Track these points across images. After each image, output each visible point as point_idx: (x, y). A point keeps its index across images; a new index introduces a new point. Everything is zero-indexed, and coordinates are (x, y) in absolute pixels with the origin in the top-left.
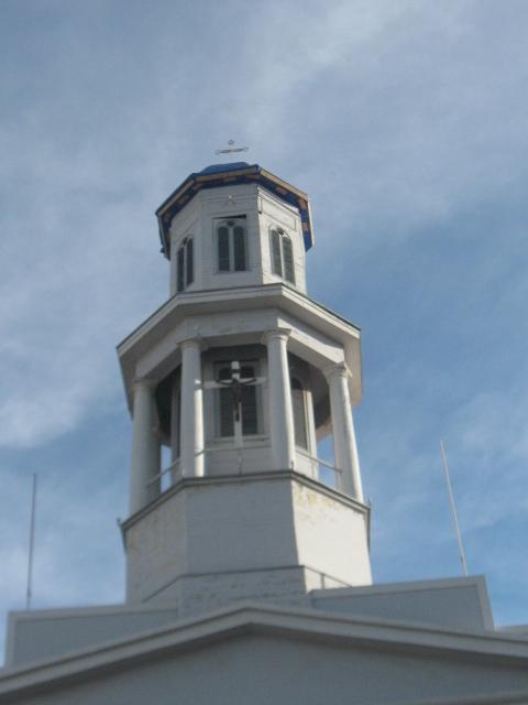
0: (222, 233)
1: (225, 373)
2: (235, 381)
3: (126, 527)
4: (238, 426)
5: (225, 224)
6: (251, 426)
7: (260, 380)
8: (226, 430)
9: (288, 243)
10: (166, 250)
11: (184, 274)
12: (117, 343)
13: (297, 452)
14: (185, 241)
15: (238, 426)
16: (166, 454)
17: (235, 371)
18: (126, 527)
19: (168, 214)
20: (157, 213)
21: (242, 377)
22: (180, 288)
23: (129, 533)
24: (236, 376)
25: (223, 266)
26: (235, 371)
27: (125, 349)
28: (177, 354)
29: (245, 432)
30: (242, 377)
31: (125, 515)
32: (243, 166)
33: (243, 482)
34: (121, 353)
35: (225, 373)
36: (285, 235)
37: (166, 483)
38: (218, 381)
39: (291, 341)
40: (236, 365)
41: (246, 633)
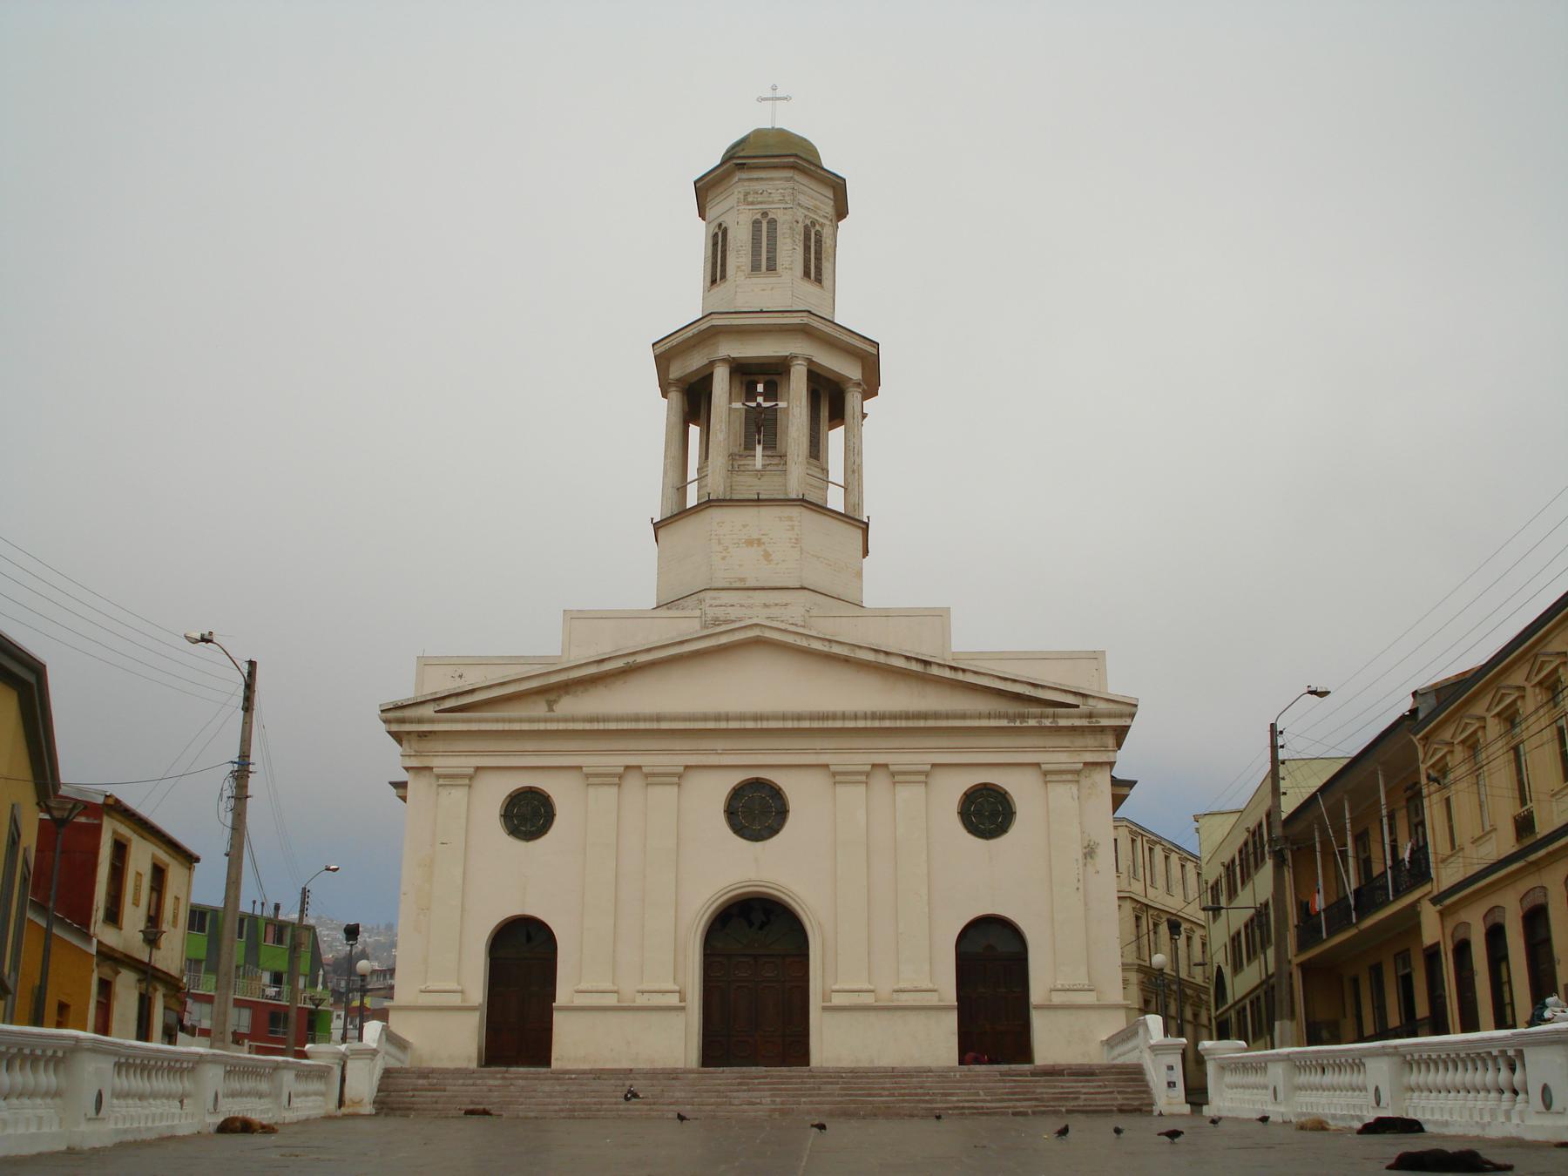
0: (756, 224)
1: (751, 394)
2: (759, 405)
3: (657, 527)
4: (759, 449)
5: (759, 216)
6: (771, 444)
7: (782, 404)
8: (749, 446)
10: (702, 214)
11: (717, 273)
14: (720, 225)
15: (759, 449)
16: (694, 431)
17: (760, 394)
18: (657, 527)
19: (706, 189)
21: (765, 401)
22: (713, 282)
23: (661, 533)
24: (760, 399)
25: (755, 267)
26: (760, 394)
27: (661, 348)
28: (712, 364)
29: (764, 448)
30: (765, 401)
32: (783, 136)
34: (658, 351)
35: (751, 394)
37: (692, 500)
38: (743, 404)
39: (810, 361)
40: (760, 388)
41: (758, 642)
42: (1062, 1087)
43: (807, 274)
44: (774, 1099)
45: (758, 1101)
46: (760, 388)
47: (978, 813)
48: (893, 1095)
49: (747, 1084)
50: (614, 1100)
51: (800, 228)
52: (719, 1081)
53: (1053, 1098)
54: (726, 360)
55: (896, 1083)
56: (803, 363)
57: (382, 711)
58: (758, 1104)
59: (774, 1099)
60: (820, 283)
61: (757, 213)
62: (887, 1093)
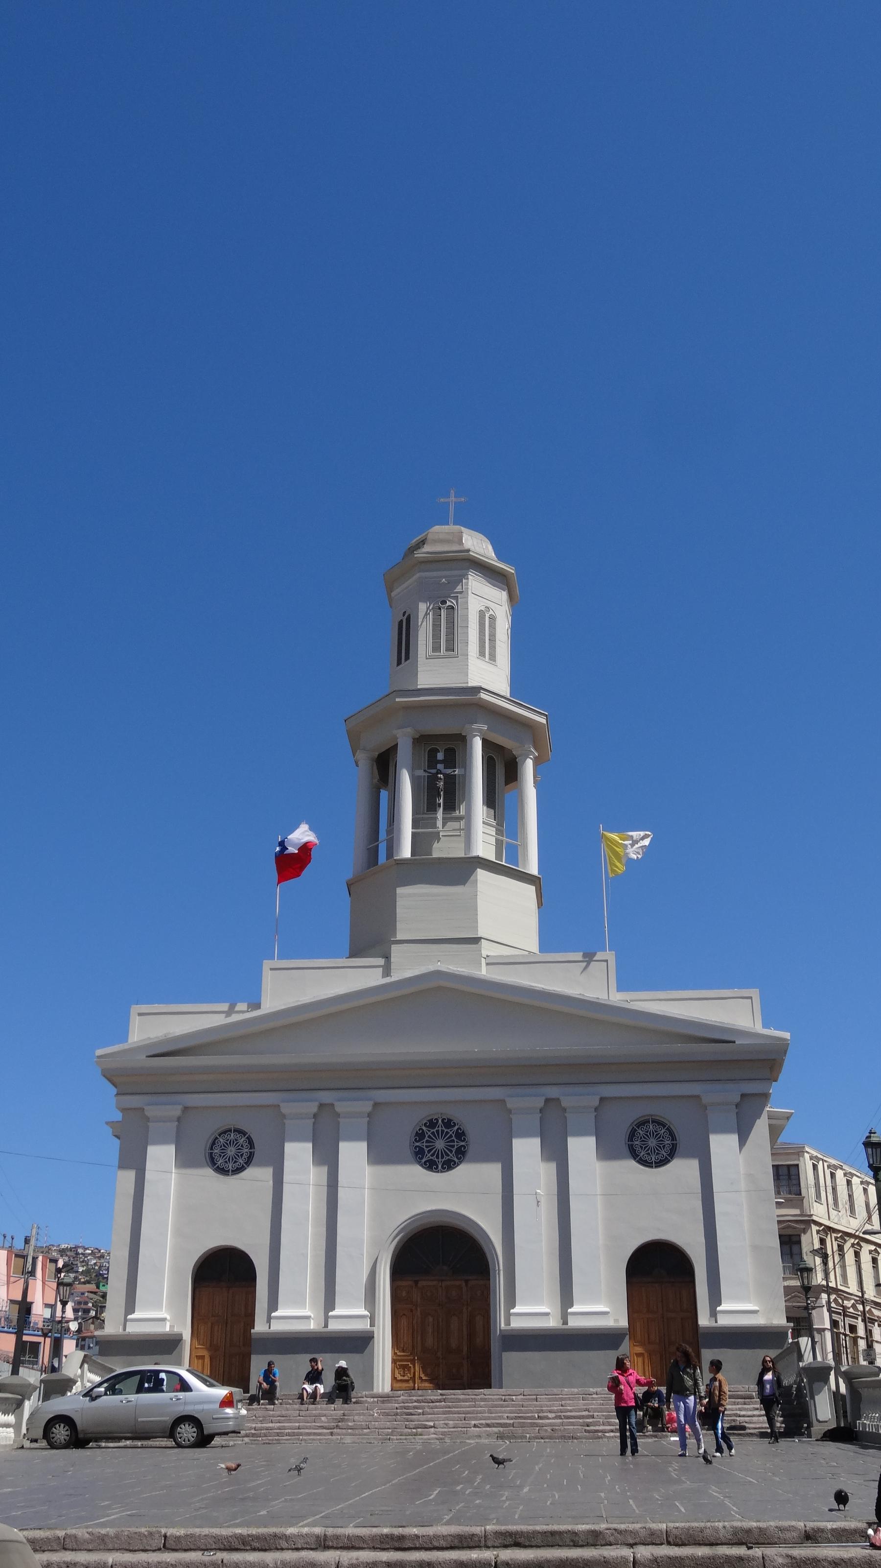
3: (349, 885)
8: (432, 807)
9: (493, 619)
24: (440, 766)
25: (436, 648)
31: (349, 875)
36: (491, 612)
40: (440, 756)
43: (482, 653)
44: (446, 1422)
45: (431, 1424)
46: (440, 756)
48: (560, 1417)
49: (423, 1408)
50: (297, 1424)
52: (396, 1405)
55: (562, 1406)
58: (431, 1427)
59: (446, 1422)
60: (495, 661)
62: (553, 1415)
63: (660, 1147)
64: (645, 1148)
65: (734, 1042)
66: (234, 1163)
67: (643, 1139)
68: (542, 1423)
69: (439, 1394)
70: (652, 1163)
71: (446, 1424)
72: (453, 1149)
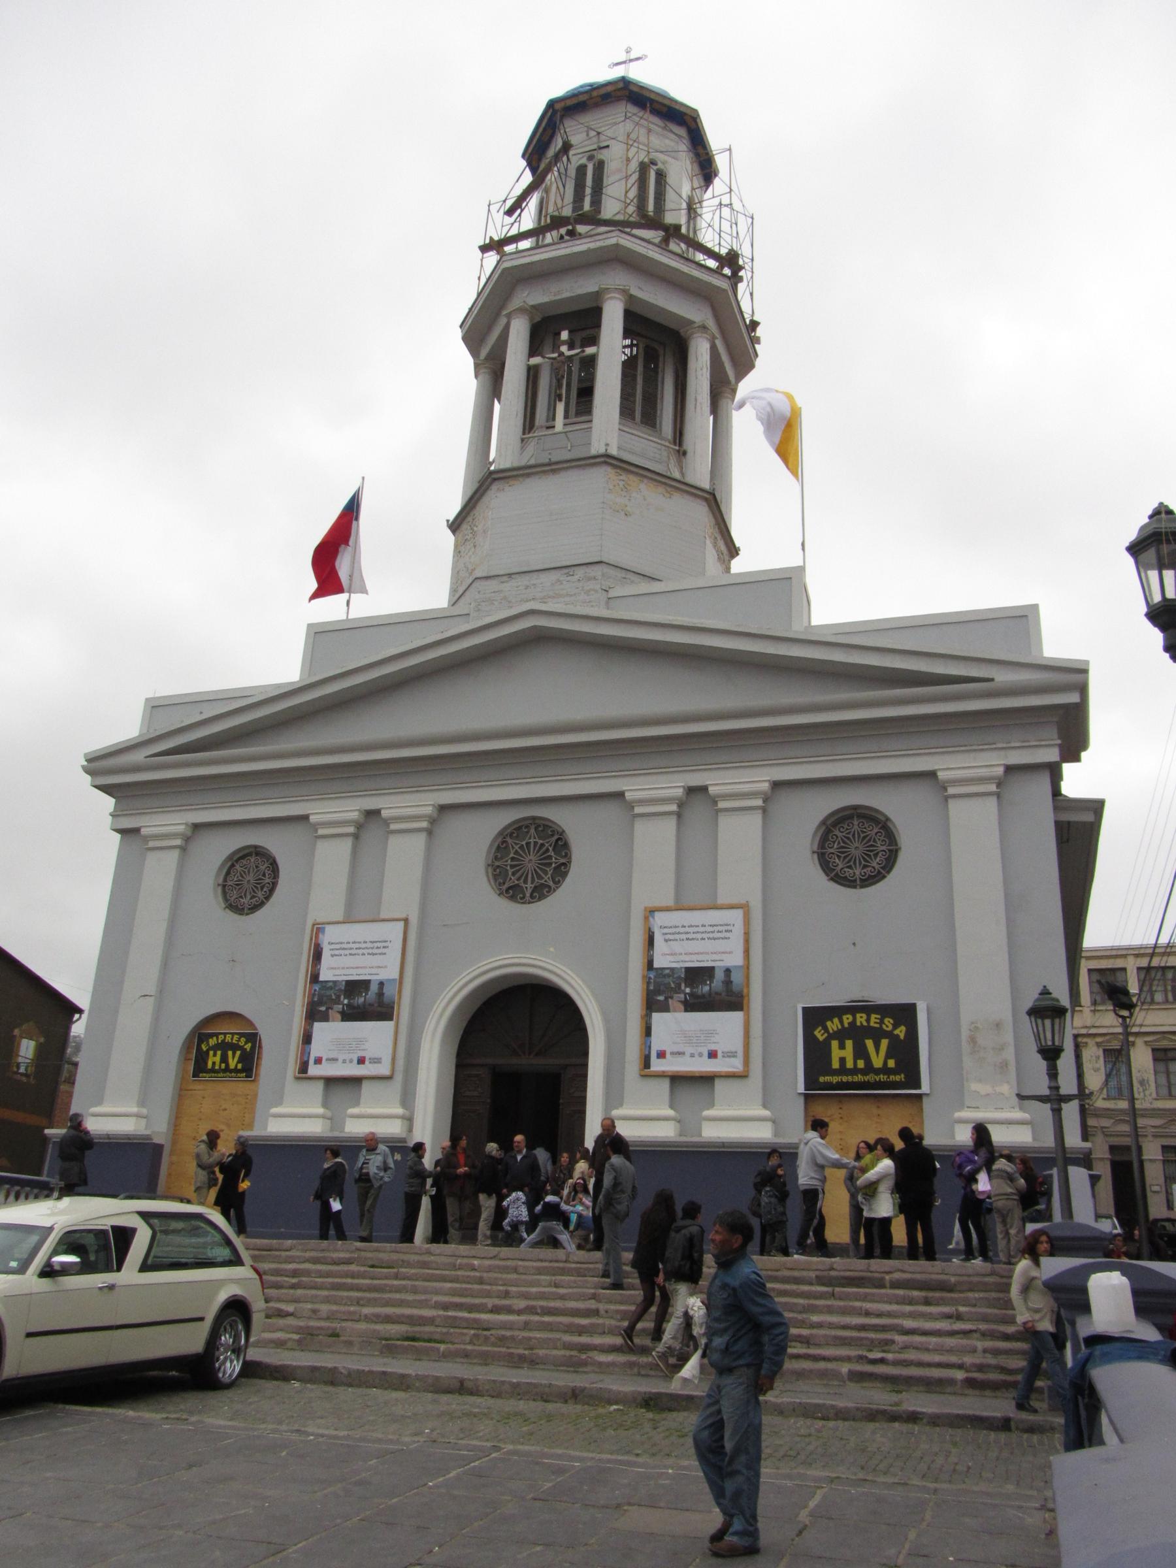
2: (561, 354)
5: (584, 161)
12: (460, 324)
13: (535, 432)
17: (564, 343)
20: (523, 156)
24: (564, 349)
26: (564, 343)
33: (554, 471)
39: (630, 299)
40: (565, 335)
42: (868, 1314)
45: (290, 1308)
46: (565, 335)
47: (843, 853)
51: (634, 165)
53: (836, 1338)
54: (521, 310)
55: (556, 1286)
56: (617, 295)
57: (89, 761)
58: (291, 1314)
61: (583, 157)
63: (869, 856)
64: (845, 858)
65: (992, 680)
66: (251, 899)
67: (842, 844)
68: (488, 1321)
69: (354, 1248)
70: (855, 880)
71: (314, 1311)
72: (548, 869)
